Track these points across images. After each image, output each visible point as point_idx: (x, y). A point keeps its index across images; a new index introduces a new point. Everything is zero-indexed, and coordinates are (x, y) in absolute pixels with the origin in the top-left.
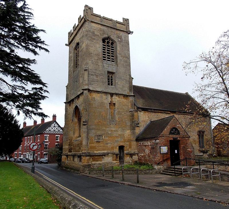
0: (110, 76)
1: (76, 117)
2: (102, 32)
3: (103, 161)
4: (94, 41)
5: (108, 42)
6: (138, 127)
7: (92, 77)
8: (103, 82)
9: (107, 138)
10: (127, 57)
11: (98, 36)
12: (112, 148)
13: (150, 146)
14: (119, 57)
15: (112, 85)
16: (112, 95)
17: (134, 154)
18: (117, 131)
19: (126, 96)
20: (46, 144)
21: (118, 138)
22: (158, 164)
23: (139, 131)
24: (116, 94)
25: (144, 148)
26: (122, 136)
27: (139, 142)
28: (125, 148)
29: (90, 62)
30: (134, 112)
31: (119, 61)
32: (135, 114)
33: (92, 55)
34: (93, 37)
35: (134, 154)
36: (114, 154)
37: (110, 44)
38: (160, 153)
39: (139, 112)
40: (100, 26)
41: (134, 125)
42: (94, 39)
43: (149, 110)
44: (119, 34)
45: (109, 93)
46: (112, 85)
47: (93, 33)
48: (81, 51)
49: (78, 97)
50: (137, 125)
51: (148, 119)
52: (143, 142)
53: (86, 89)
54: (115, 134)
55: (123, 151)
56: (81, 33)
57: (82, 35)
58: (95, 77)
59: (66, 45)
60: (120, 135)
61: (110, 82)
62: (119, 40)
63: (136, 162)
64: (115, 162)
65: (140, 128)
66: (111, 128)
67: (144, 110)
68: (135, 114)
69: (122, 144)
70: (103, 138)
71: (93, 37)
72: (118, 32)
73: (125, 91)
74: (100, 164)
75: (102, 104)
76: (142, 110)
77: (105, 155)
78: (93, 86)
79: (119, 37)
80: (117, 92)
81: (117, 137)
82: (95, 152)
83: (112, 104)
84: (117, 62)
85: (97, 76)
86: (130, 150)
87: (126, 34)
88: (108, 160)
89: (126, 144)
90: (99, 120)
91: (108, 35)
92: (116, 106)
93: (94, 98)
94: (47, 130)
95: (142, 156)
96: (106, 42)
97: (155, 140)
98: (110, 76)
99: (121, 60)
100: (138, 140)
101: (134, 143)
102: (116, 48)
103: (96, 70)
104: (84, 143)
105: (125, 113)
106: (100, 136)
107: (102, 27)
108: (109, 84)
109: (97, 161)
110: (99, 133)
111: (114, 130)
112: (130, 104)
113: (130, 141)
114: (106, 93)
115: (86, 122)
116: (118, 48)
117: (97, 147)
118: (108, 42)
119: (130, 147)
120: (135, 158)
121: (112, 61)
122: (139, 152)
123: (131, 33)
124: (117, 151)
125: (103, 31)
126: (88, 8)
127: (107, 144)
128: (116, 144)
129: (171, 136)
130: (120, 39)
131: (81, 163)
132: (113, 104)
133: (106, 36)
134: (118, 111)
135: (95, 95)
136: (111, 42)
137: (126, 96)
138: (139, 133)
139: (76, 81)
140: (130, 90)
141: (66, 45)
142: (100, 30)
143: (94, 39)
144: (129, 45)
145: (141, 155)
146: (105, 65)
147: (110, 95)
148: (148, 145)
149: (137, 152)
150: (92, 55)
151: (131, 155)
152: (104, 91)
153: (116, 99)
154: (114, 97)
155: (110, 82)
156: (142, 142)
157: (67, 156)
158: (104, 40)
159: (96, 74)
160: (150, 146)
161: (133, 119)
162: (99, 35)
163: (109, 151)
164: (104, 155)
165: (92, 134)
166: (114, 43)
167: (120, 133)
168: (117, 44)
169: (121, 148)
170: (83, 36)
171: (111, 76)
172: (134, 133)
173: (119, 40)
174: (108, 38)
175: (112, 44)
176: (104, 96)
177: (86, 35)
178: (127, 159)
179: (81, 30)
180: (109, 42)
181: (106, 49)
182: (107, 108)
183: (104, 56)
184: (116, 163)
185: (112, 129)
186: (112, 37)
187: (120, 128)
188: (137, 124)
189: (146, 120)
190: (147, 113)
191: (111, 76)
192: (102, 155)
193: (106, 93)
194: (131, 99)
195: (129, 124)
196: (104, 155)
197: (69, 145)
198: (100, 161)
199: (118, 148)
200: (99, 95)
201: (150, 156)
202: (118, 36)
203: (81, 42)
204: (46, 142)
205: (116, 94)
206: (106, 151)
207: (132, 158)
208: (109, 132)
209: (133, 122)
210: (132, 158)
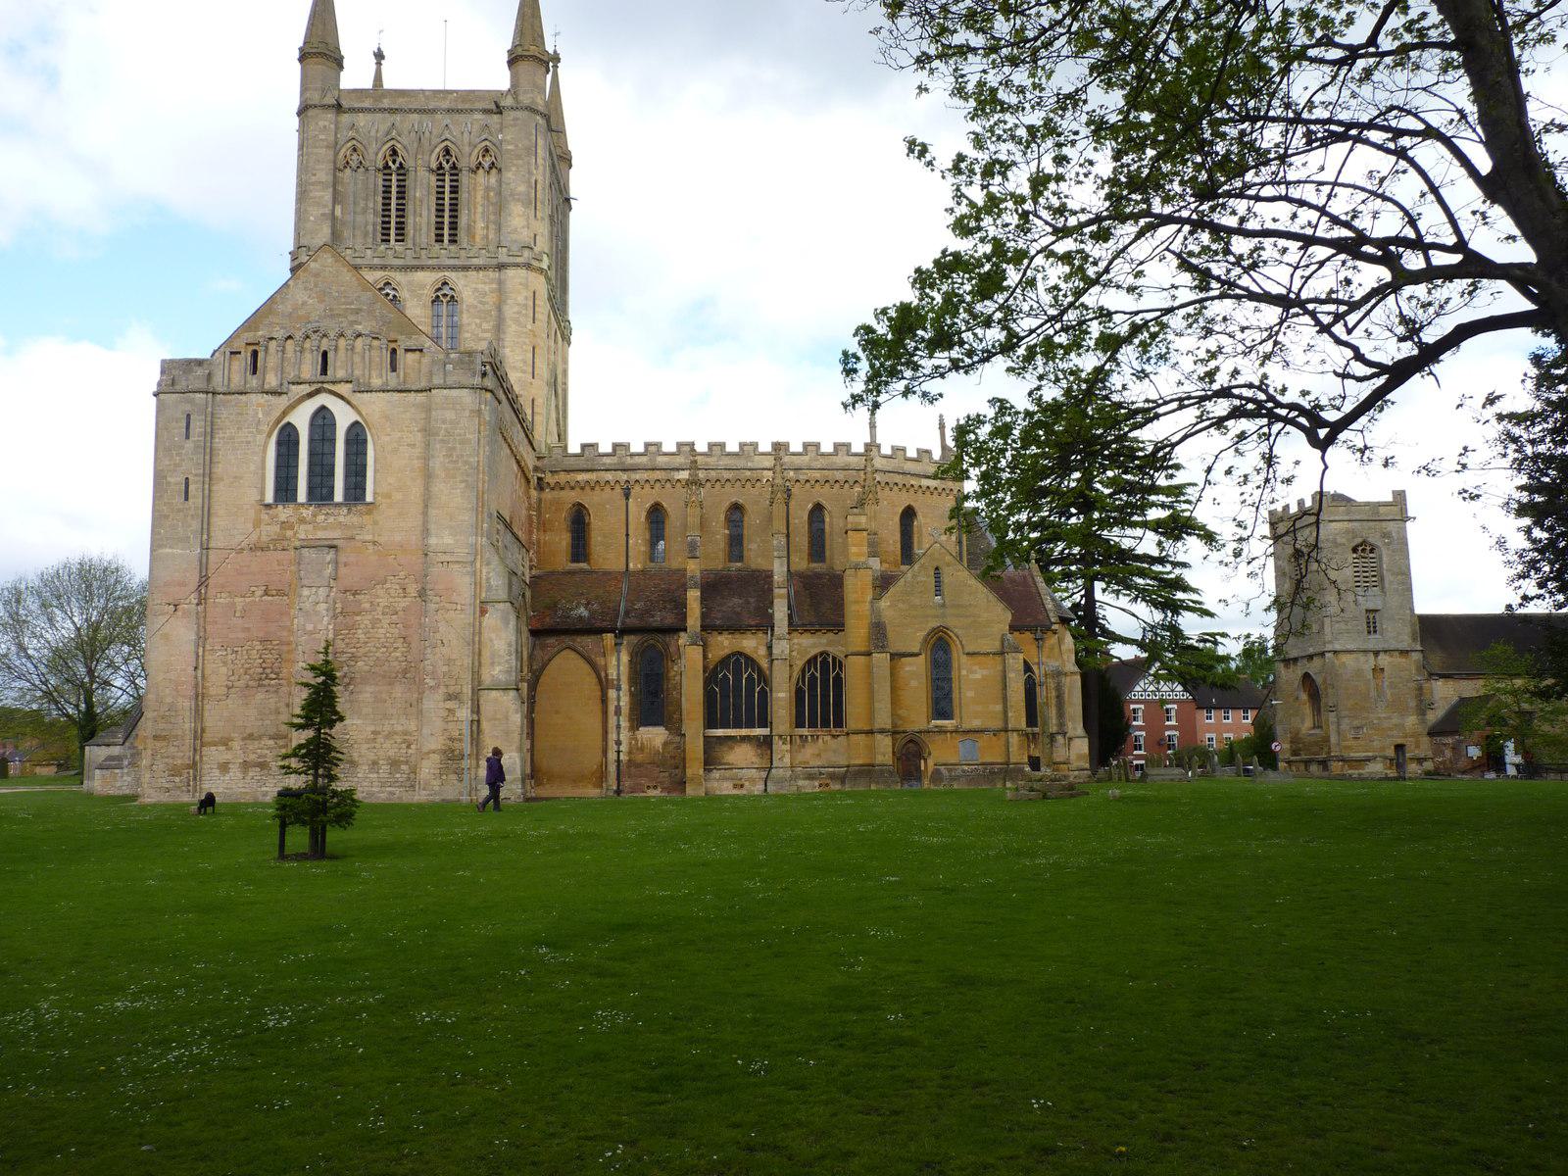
0: (1371, 616)
10: (1403, 574)
12: (1383, 749)
14: (1388, 577)
15: (1375, 632)
16: (1376, 653)
17: (1425, 759)
18: (1389, 718)
20: (1137, 733)
22: (1464, 773)
23: (1432, 717)
26: (1401, 727)
28: (1407, 749)
31: (1387, 585)
32: (1426, 685)
35: (1425, 759)
36: (1386, 758)
41: (1423, 706)
46: (1375, 632)
47: (1335, 542)
49: (1310, 657)
50: (1431, 706)
54: (1386, 725)
55: (1404, 754)
61: (1372, 628)
69: (1399, 741)
72: (1384, 524)
75: (1359, 673)
77: (1369, 760)
81: (1391, 729)
82: (1352, 755)
83: (1378, 671)
84: (1383, 588)
85: (1346, 623)
88: (1377, 768)
89: (1409, 742)
92: (1386, 674)
94: (1138, 688)
98: (1371, 616)
99: (1391, 582)
100: (1432, 733)
101: (1425, 740)
102: (1381, 558)
104: (1333, 739)
107: (1351, 524)
108: (1369, 632)
110: (1356, 723)
112: (1413, 668)
116: (1385, 559)
119: (1417, 747)
120: (1429, 765)
122: (1436, 754)
124: (1391, 752)
125: (1353, 531)
128: (1388, 741)
130: (1389, 538)
133: (1360, 540)
135: (1345, 658)
137: (1404, 653)
140: (1414, 640)
142: (1347, 531)
144: (1407, 545)
151: (1420, 761)
153: (1384, 660)
154: (1382, 656)
155: (1372, 628)
157: (1289, 762)
164: (1368, 760)
165: (1345, 724)
167: (1395, 721)
169: (1399, 748)
172: (1423, 721)
174: (1364, 543)
176: (1362, 657)
178: (1413, 768)
186: (1370, 540)
190: (1451, 683)
195: (1413, 704)
196: (1368, 760)
200: (1354, 655)
204: (1140, 728)
206: (1370, 754)
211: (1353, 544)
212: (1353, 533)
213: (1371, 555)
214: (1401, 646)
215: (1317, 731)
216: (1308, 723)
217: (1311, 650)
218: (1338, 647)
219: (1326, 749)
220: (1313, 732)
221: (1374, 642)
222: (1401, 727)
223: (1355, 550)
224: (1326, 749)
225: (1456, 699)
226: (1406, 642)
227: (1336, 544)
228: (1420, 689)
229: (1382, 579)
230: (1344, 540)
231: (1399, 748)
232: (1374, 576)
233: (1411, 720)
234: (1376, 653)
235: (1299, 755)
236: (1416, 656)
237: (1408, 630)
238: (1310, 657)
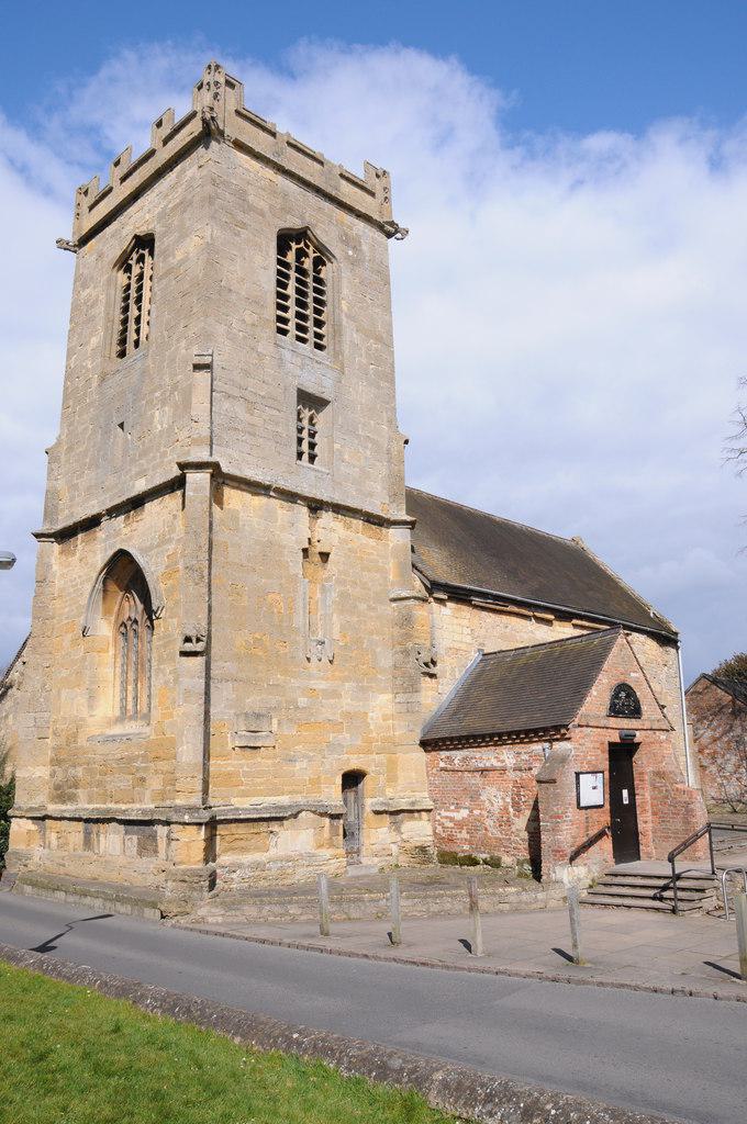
1: (107, 612)
3: (273, 852)
4: (244, 234)
5: (301, 254)
6: (432, 676)
7: (226, 405)
9: (290, 731)
10: (379, 339)
11: (262, 214)
12: (316, 782)
13: (511, 775)
14: (350, 335)
15: (312, 458)
16: (316, 506)
18: (335, 694)
21: (340, 731)
23: (436, 696)
24: (338, 509)
25: (477, 779)
27: (444, 754)
29: (221, 329)
30: (411, 602)
31: (346, 349)
33: (233, 297)
34: (241, 216)
37: (308, 264)
38: (579, 807)
39: (435, 605)
40: (269, 173)
42: (244, 225)
43: (477, 600)
44: (349, 227)
45: (304, 498)
47: (242, 195)
48: (167, 273)
49: (136, 503)
51: (468, 639)
52: (465, 753)
53: (199, 466)
56: (173, 188)
57: (176, 198)
58: (240, 410)
59: (63, 245)
60: (348, 716)
61: (307, 451)
62: (350, 253)
63: (423, 849)
64: (326, 853)
65: (438, 683)
66: (310, 677)
67: (460, 596)
68: (420, 612)
70: (275, 727)
71: (241, 216)
73: (371, 495)
74: (258, 866)
75: (269, 551)
76: (451, 599)
78: (229, 451)
79: (348, 240)
80: (338, 499)
81: (336, 726)
82: (237, 802)
84: (337, 354)
85: (251, 406)
86: (389, 792)
87: (380, 237)
90: (257, 636)
91: (302, 218)
95: (460, 825)
96: (290, 248)
97: (545, 741)
103: (247, 373)
105: (370, 608)
106: (258, 716)
108: (300, 455)
109: (244, 850)
110: (253, 701)
111: (321, 687)
112: (391, 565)
113: (390, 746)
114: (290, 497)
115: (198, 640)
117: (246, 774)
118: (301, 254)
119: (392, 779)
120: (419, 831)
122: (440, 802)
123: (399, 235)
124: (333, 795)
125: (285, 195)
126: (222, 80)
127: (292, 760)
129: (614, 722)
131: (149, 864)
132: (321, 554)
133: (294, 223)
136: (312, 255)
138: (435, 708)
139: (121, 426)
140: (394, 496)
141: (63, 245)
142: (273, 190)
143: (244, 225)
145: (452, 819)
146: (287, 355)
147: (309, 507)
148: (504, 770)
149: (429, 804)
150: (233, 297)
152: (282, 484)
158: (285, 240)
159: (247, 395)
160: (511, 775)
161: (408, 636)
162: (268, 214)
163: (300, 799)
166: (324, 264)
167: (346, 703)
168: (339, 269)
170: (184, 205)
171: (311, 419)
172: (410, 709)
173: (350, 253)
174: (302, 235)
175: (318, 262)
177: (211, 200)
178: (379, 839)
179: (171, 177)
180: (307, 255)
182: (292, 572)
184: (332, 860)
185: (314, 684)
187: (347, 679)
188: (426, 664)
189: (464, 647)
190: (465, 611)
191: (311, 419)
193: (290, 497)
194: (399, 537)
195: (386, 659)
197: (56, 762)
198: (257, 849)
199: (339, 781)
200: (259, 501)
201: (509, 823)
202: (346, 235)
203: (165, 234)
205: (338, 509)
206: (284, 800)
207: (398, 830)
208: (302, 701)
209: (406, 653)
210: (398, 830)
215: (131, 727)
216: (108, 705)
219: (155, 783)
220: (117, 730)
221: (307, 481)
222: (355, 719)
224: (155, 783)
225: (474, 657)
228: (407, 621)
230: (262, 205)
233: (382, 704)
235: (72, 798)
238: (136, 503)
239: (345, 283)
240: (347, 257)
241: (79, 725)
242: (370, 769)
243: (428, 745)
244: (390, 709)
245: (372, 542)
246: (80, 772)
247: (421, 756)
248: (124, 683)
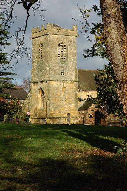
2: (58, 40)
4: (53, 47)
8: (59, 74)
18: (66, 104)
19: (72, 82)
28: (71, 115)
31: (69, 58)
32: (78, 93)
42: (53, 46)
47: (53, 41)
49: (42, 82)
55: (70, 117)
58: (54, 72)
61: (63, 73)
68: (78, 93)
69: (68, 113)
72: (69, 37)
79: (70, 41)
83: (63, 88)
86: (74, 116)
93: (53, 85)
99: (70, 58)
100: (78, 110)
102: (67, 49)
106: (56, 107)
110: (55, 106)
116: (69, 49)
121: (64, 59)
124: (66, 116)
127: (60, 112)
129: (96, 109)
134: (67, 92)
140: (76, 78)
143: (53, 46)
153: (66, 84)
156: (81, 112)
165: (52, 106)
167: (68, 105)
169: (68, 114)
172: (76, 106)
181: (61, 51)
183: (59, 54)
187: (68, 102)
192: (57, 119)
197: (34, 112)
200: (56, 82)
205: (67, 81)
208: (62, 105)
210: (75, 121)
211: (59, 43)
212: (59, 39)
213: (64, 48)
214: (71, 80)
217: (43, 80)
218: (51, 79)
221: (62, 78)
222: (69, 108)
223: (59, 45)
226: (73, 78)
227: (53, 43)
229: (67, 55)
231: (68, 114)
232: (65, 56)
233: (73, 105)
234: (64, 82)
235: (36, 116)
236: (76, 84)
237: (74, 75)
238: (42, 82)
239: (69, 48)
240: (69, 44)
241: (37, 107)
242: (71, 113)
243: (78, 110)
244: (74, 106)
245: (72, 85)
246: (37, 113)
247: (78, 112)
248: (42, 103)
